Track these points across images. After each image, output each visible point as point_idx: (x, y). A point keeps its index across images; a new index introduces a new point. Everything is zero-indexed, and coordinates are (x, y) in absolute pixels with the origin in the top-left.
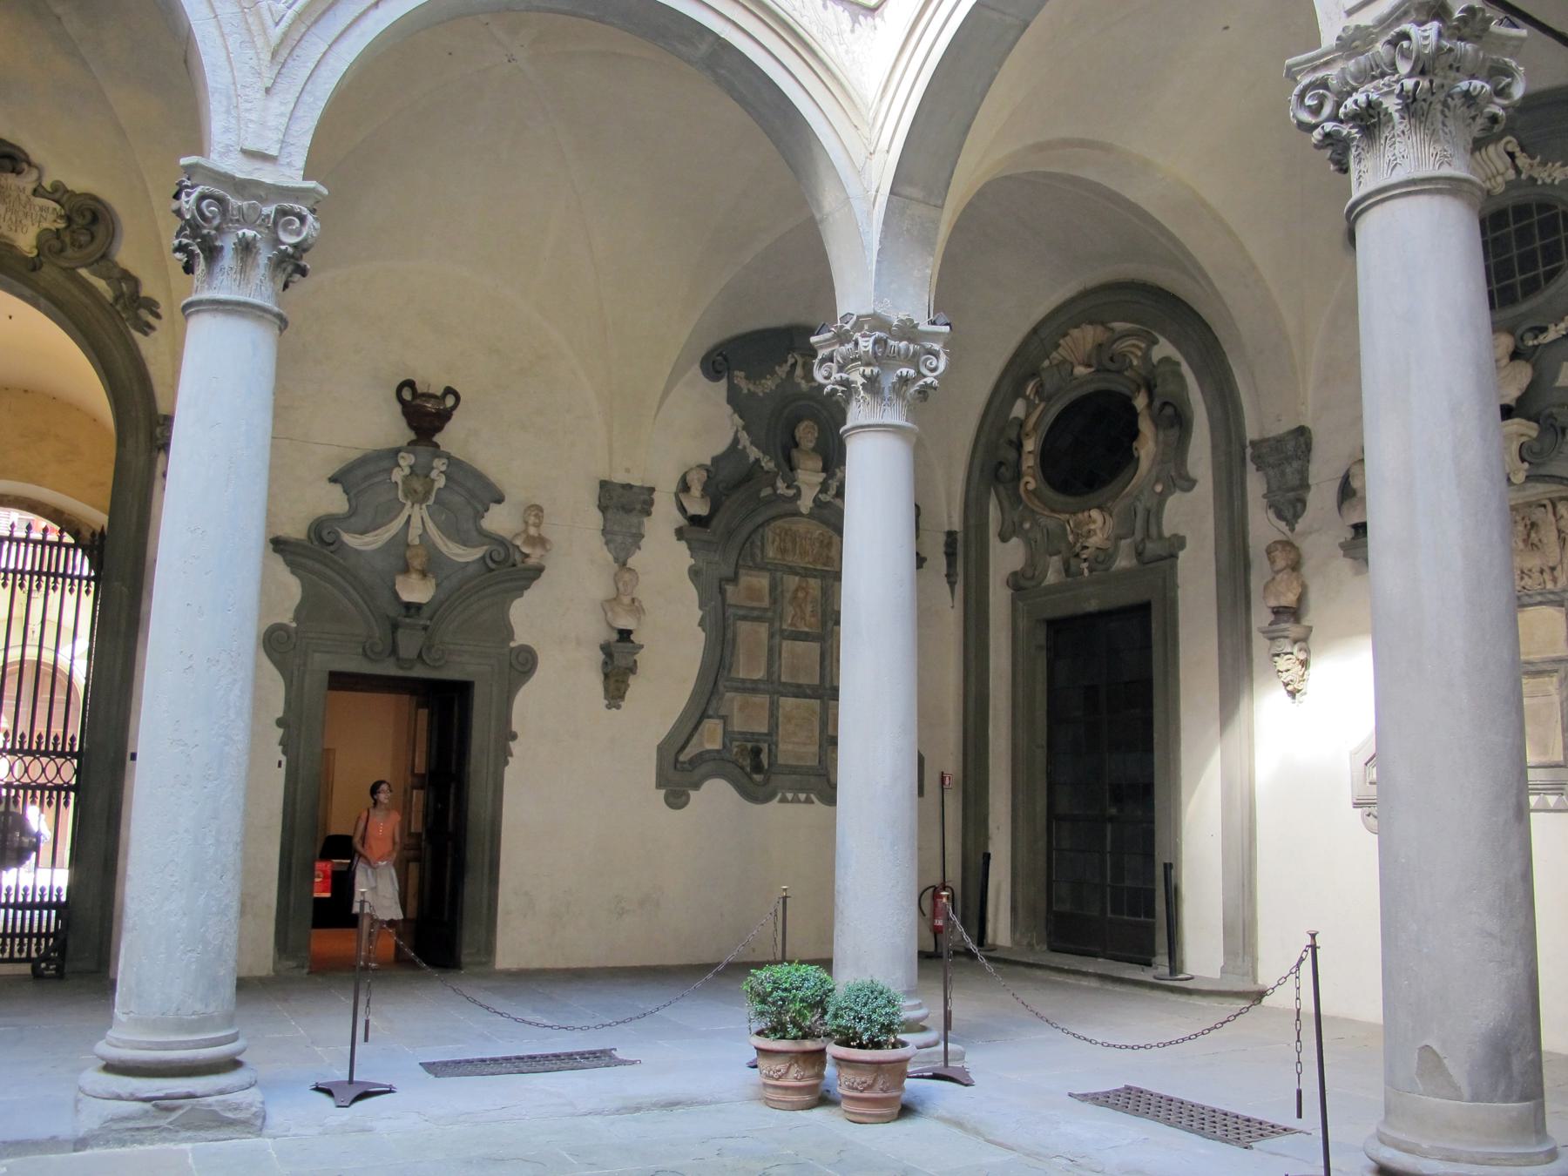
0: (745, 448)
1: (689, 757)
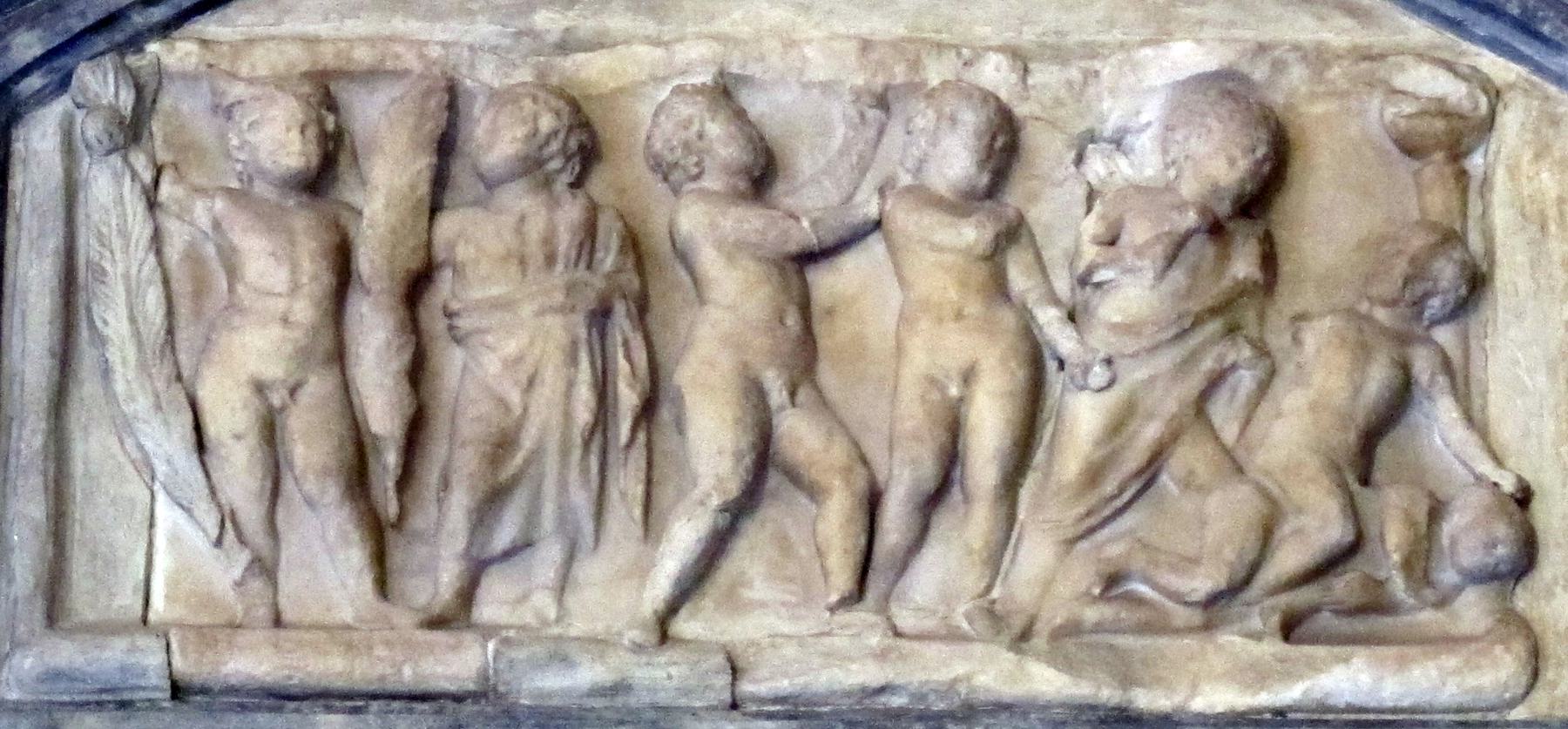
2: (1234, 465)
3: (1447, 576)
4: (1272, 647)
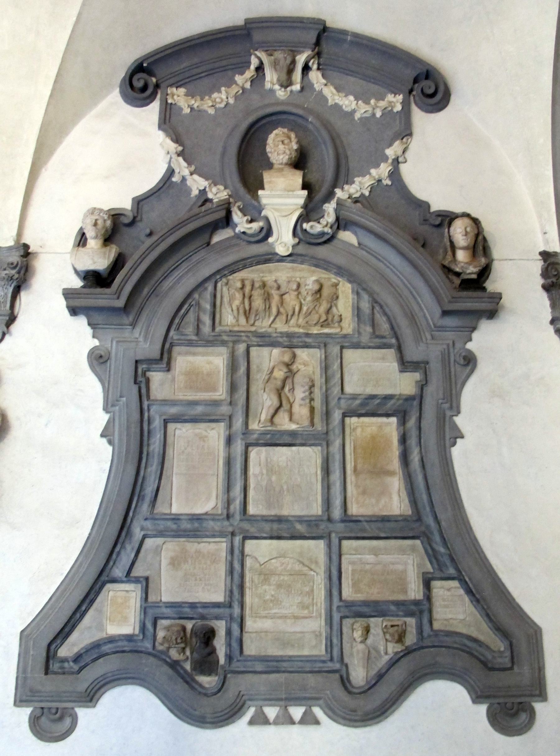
0: (184, 179)
1: (76, 650)
2: (317, 313)
3: (335, 322)
4: (320, 328)
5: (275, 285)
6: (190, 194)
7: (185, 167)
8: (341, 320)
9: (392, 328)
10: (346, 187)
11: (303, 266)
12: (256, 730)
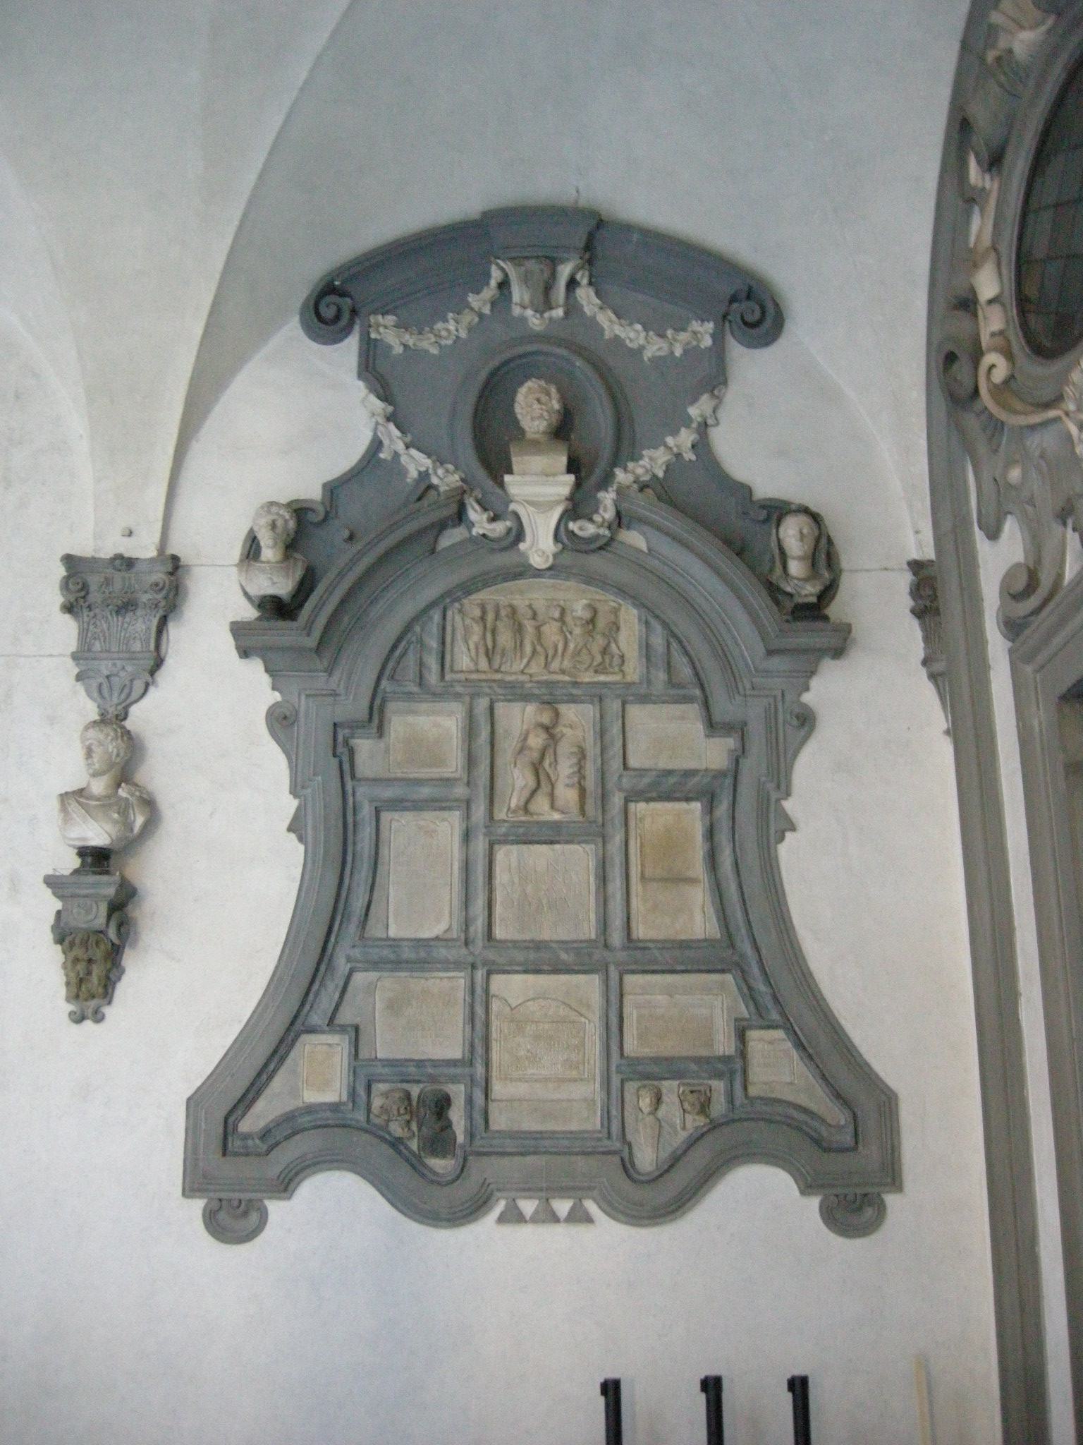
0: (396, 455)
1: (262, 1124)
5: (530, 613)
6: (406, 477)
7: (398, 437)
8: (623, 661)
9: (697, 674)
10: (631, 465)
11: (568, 583)
12: (507, 1230)
